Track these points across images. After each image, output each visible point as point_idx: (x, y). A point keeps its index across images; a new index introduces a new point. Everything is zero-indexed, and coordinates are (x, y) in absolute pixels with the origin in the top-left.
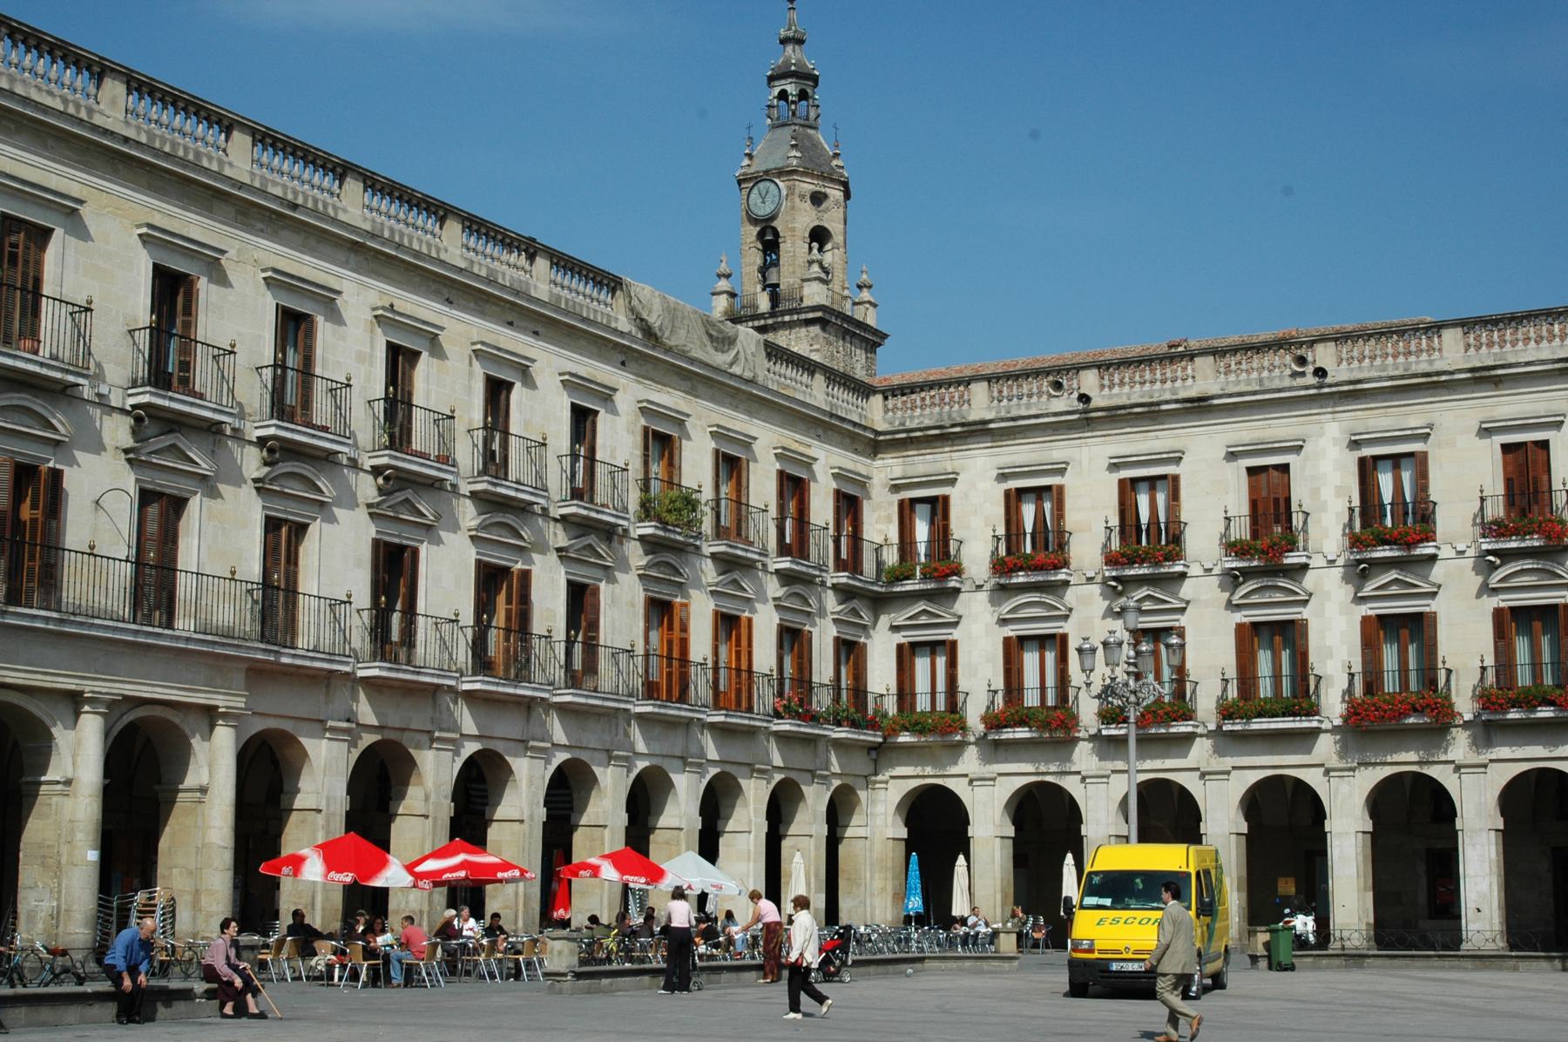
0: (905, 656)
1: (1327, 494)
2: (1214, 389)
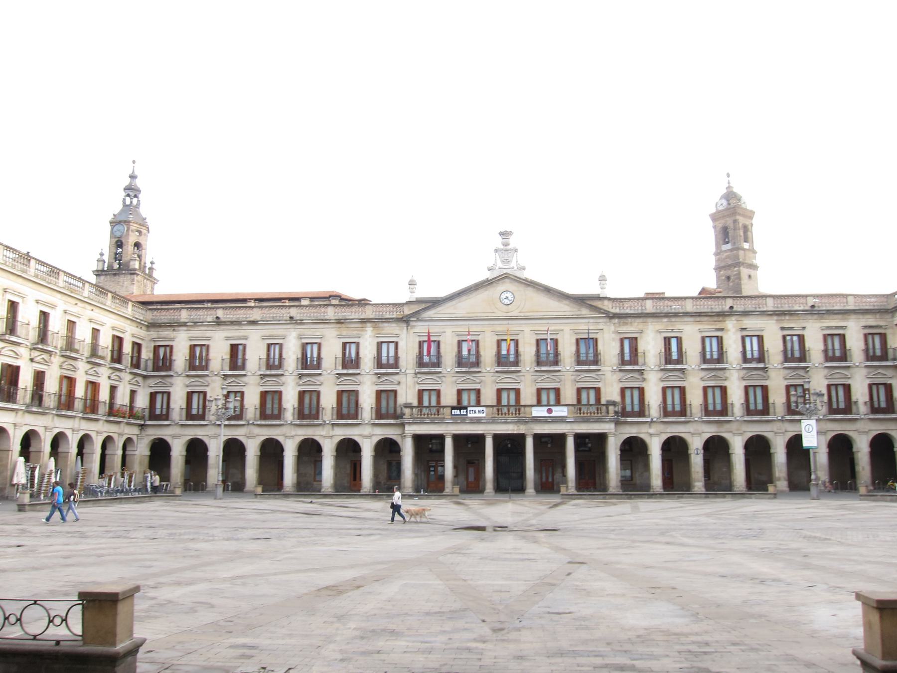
0: (153, 396)
1: (291, 353)
2: (259, 319)
